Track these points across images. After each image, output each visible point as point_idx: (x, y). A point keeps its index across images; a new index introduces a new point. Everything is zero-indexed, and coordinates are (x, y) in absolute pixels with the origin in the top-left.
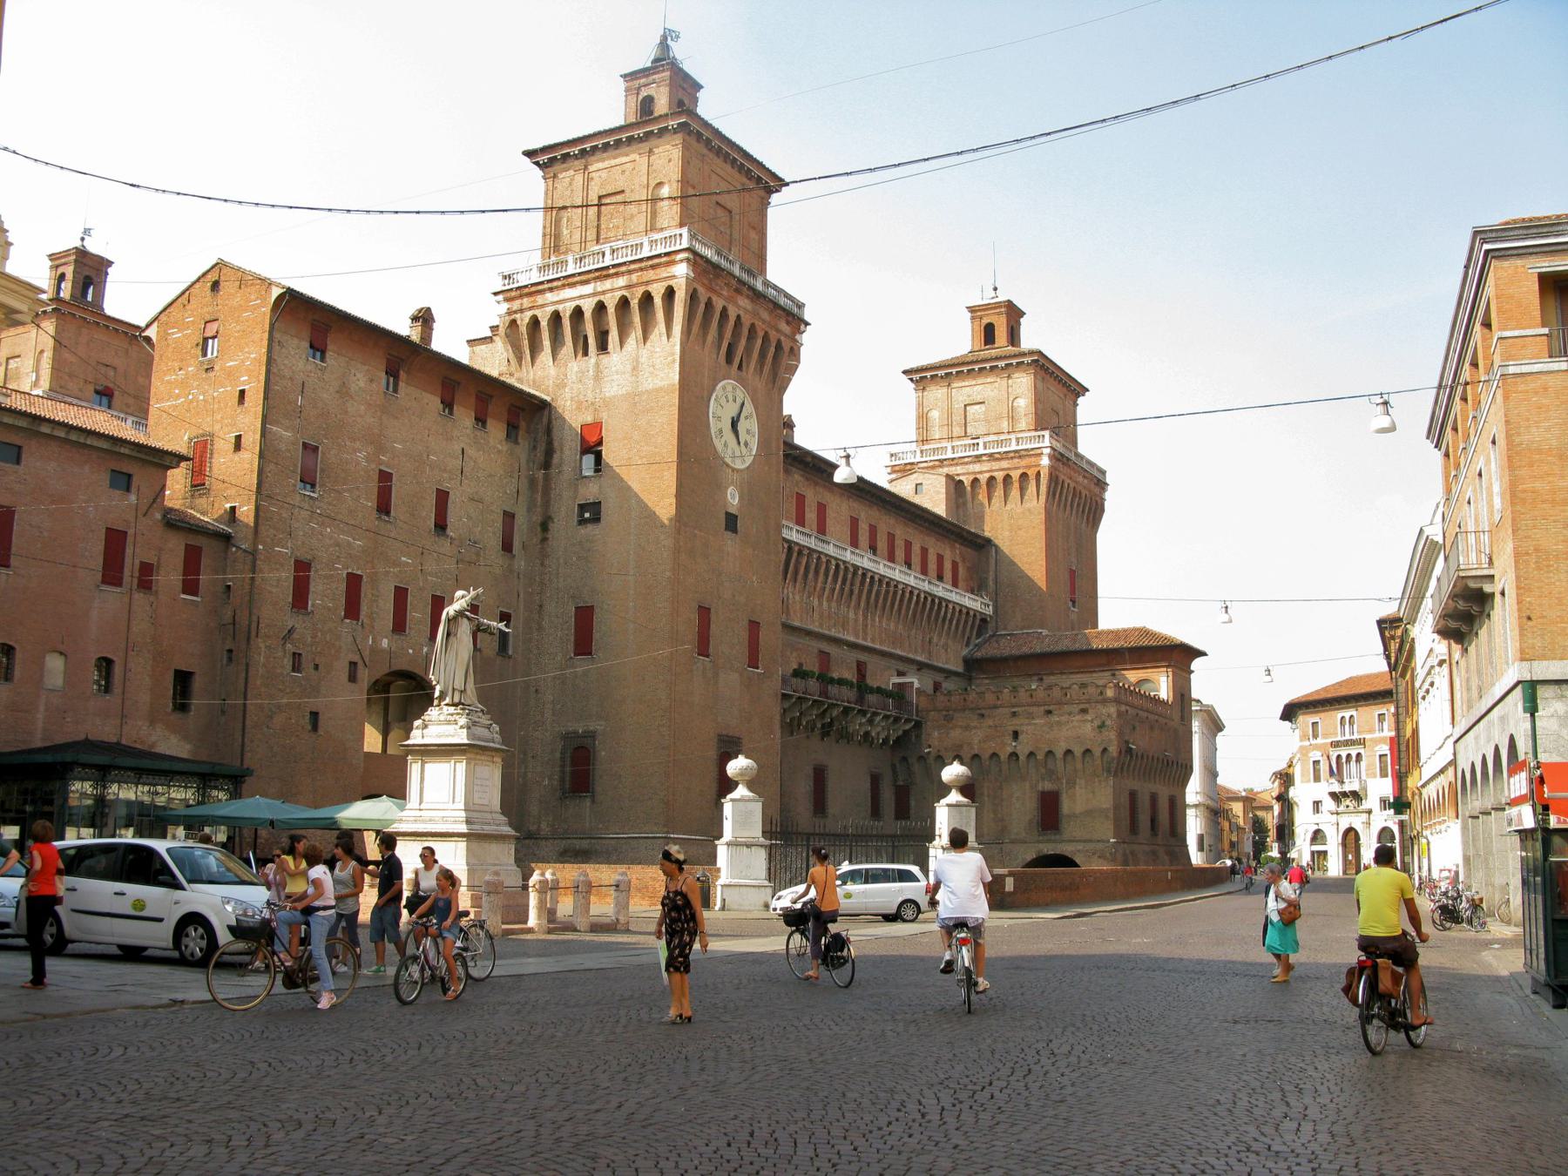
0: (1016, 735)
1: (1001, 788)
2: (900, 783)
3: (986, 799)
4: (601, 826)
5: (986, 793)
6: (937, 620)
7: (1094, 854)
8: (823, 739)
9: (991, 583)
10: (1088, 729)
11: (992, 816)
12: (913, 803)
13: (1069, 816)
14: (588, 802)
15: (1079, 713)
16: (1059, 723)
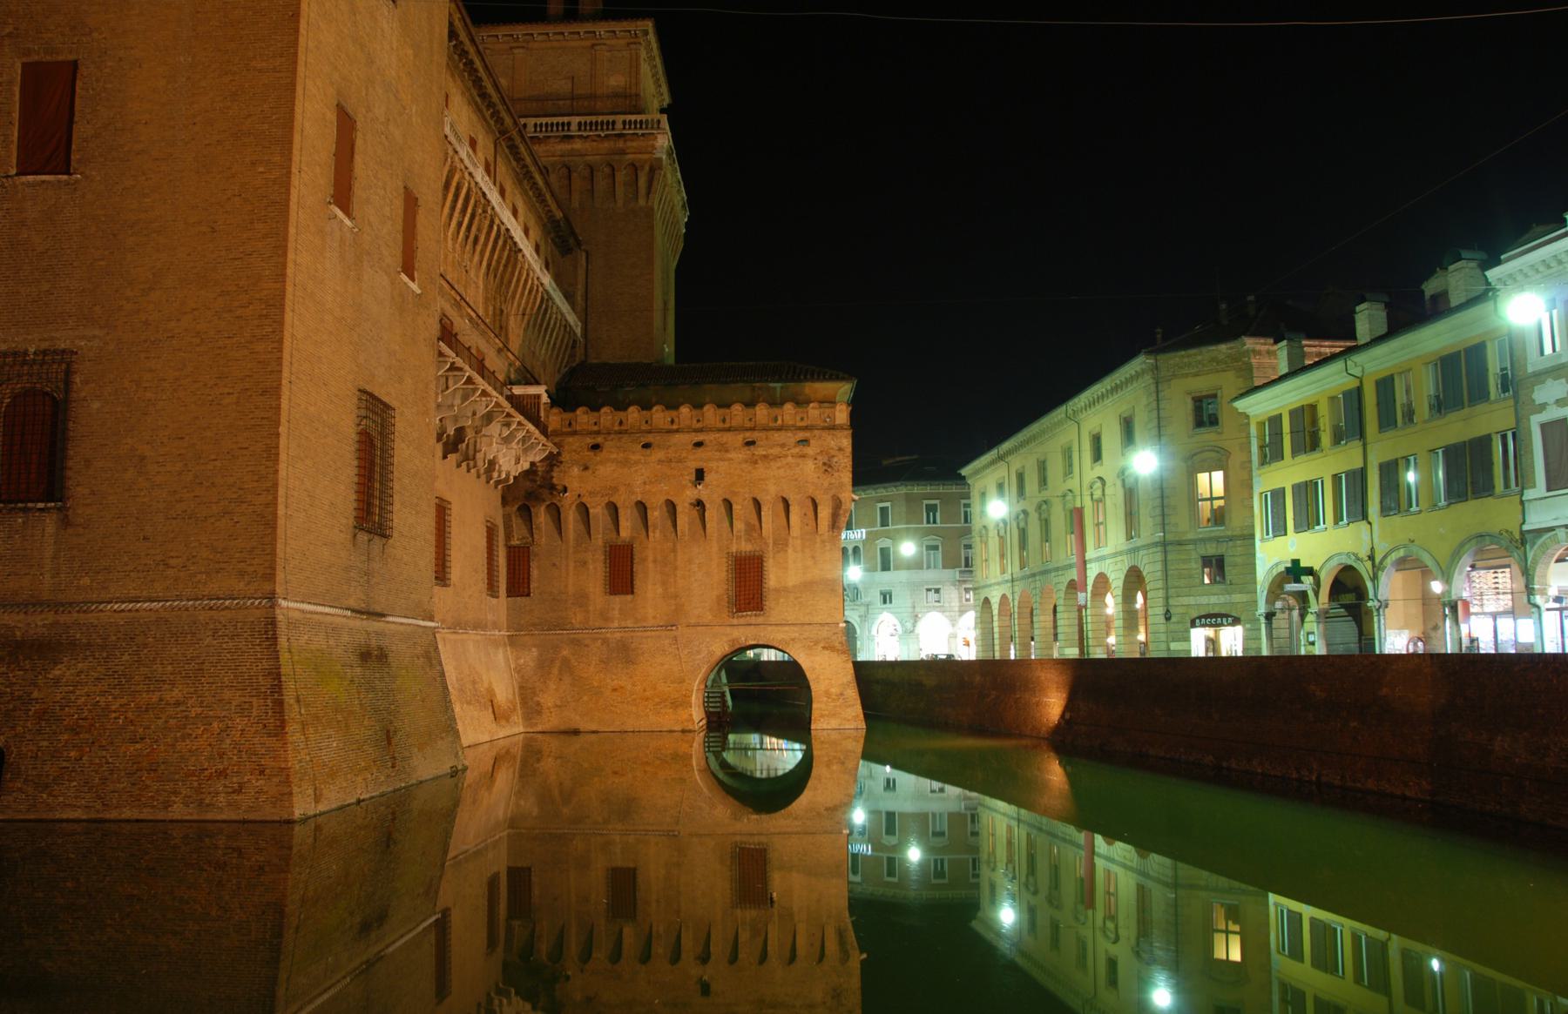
0: (700, 475)
1: (674, 551)
2: (515, 542)
3: (651, 565)
4: (86, 581)
5: (651, 558)
6: (541, 325)
7: (816, 643)
8: (445, 457)
9: (579, 298)
10: (809, 467)
11: (660, 590)
12: (535, 573)
13: (777, 590)
14: (50, 524)
15: (795, 446)
16: (765, 457)
